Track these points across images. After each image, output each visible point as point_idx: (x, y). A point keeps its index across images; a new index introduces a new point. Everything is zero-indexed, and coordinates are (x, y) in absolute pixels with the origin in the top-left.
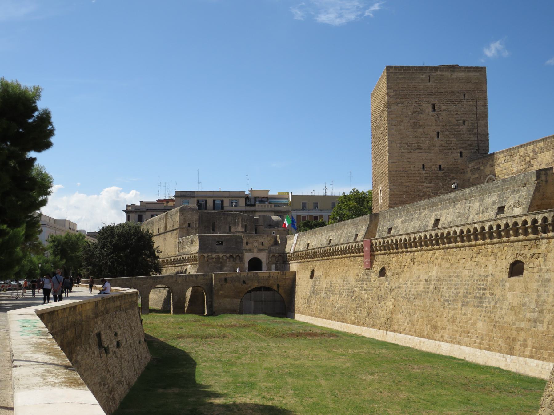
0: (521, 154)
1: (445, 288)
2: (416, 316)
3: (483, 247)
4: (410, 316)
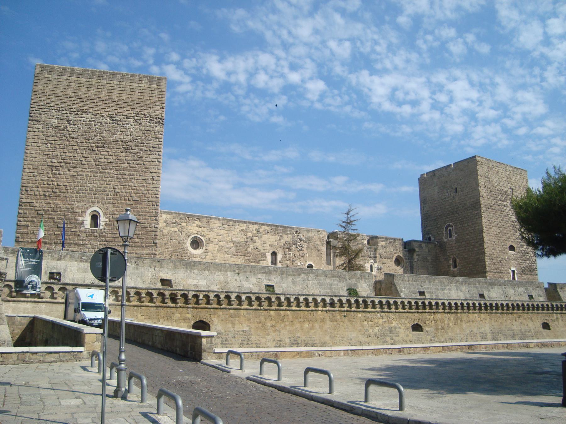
0: (244, 228)
3: (521, 314)
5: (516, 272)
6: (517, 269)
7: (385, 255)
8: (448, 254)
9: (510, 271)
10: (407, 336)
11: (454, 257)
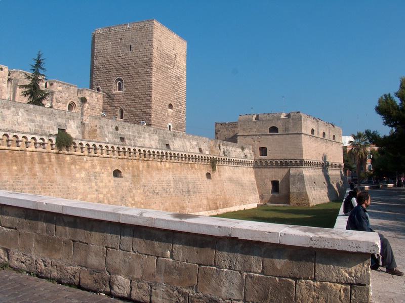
1: (181, 185)
2: (167, 204)
4: (162, 204)
5: (172, 127)
6: (172, 125)
7: (61, 99)
8: (116, 105)
9: (168, 126)
10: (110, 182)
11: (121, 109)
